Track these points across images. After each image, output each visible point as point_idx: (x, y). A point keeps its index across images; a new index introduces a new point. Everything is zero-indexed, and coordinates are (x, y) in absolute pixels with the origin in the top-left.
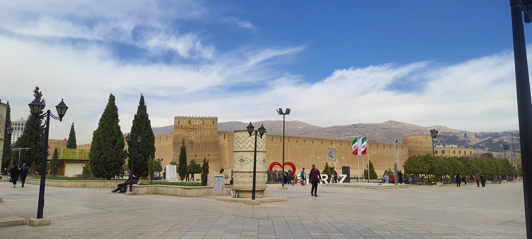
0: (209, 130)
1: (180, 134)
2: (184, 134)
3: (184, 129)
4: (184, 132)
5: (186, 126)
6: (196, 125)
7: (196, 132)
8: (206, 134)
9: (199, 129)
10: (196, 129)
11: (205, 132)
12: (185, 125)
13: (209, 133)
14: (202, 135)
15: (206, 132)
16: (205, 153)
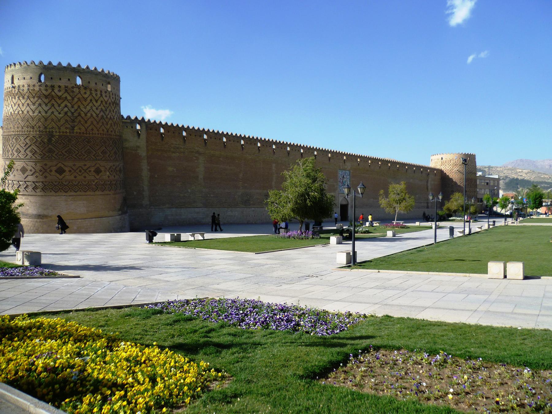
0: (97, 105)
1: (16, 112)
2: (25, 112)
3: (26, 97)
4: (26, 105)
5: (31, 88)
6: (60, 87)
7: (59, 106)
8: (89, 115)
9: (69, 98)
10: (60, 98)
11: (85, 108)
12: (29, 86)
13: (98, 112)
14: (76, 114)
15: (88, 108)
16: (85, 165)
